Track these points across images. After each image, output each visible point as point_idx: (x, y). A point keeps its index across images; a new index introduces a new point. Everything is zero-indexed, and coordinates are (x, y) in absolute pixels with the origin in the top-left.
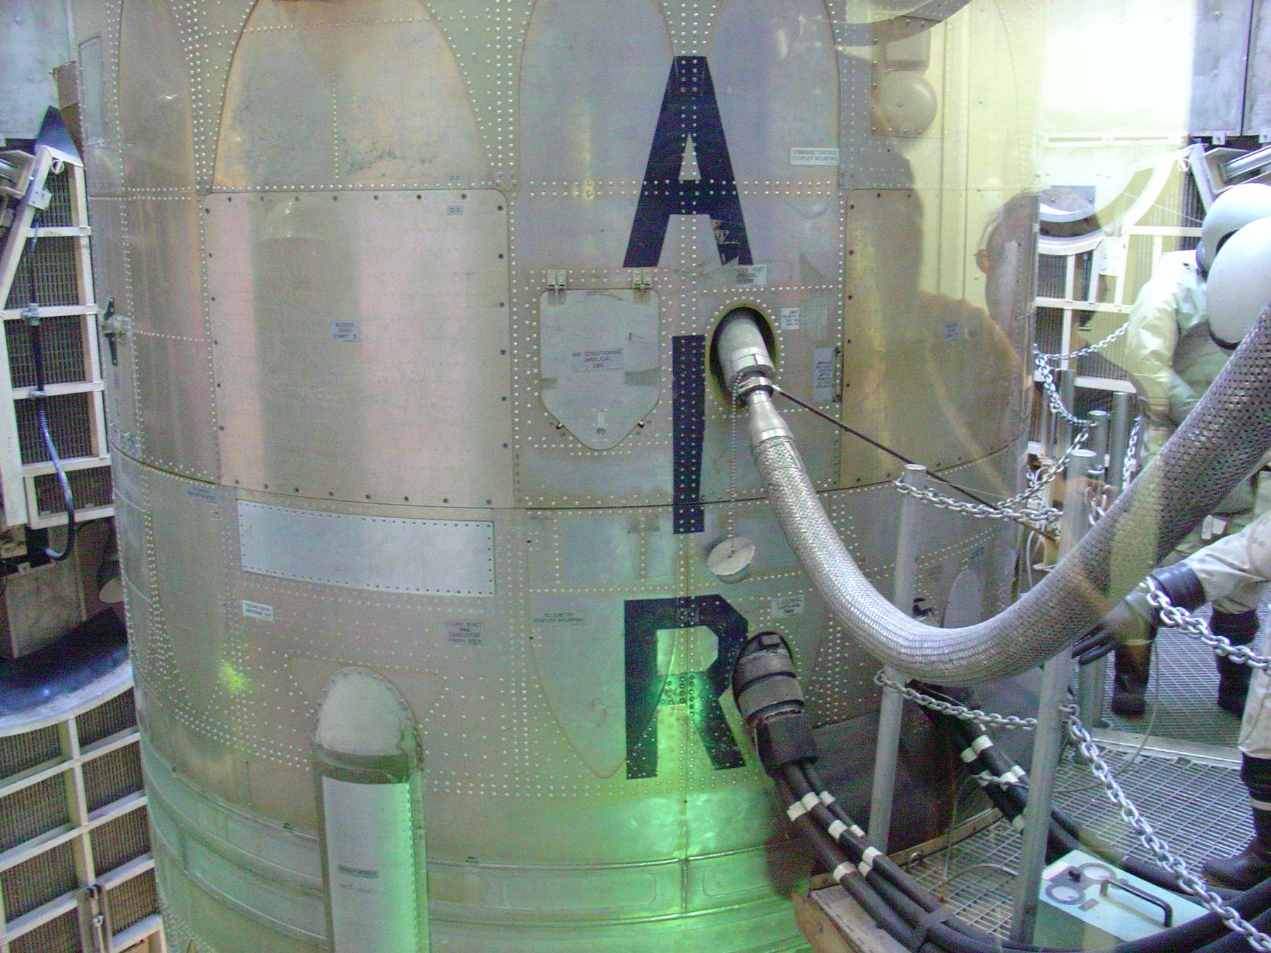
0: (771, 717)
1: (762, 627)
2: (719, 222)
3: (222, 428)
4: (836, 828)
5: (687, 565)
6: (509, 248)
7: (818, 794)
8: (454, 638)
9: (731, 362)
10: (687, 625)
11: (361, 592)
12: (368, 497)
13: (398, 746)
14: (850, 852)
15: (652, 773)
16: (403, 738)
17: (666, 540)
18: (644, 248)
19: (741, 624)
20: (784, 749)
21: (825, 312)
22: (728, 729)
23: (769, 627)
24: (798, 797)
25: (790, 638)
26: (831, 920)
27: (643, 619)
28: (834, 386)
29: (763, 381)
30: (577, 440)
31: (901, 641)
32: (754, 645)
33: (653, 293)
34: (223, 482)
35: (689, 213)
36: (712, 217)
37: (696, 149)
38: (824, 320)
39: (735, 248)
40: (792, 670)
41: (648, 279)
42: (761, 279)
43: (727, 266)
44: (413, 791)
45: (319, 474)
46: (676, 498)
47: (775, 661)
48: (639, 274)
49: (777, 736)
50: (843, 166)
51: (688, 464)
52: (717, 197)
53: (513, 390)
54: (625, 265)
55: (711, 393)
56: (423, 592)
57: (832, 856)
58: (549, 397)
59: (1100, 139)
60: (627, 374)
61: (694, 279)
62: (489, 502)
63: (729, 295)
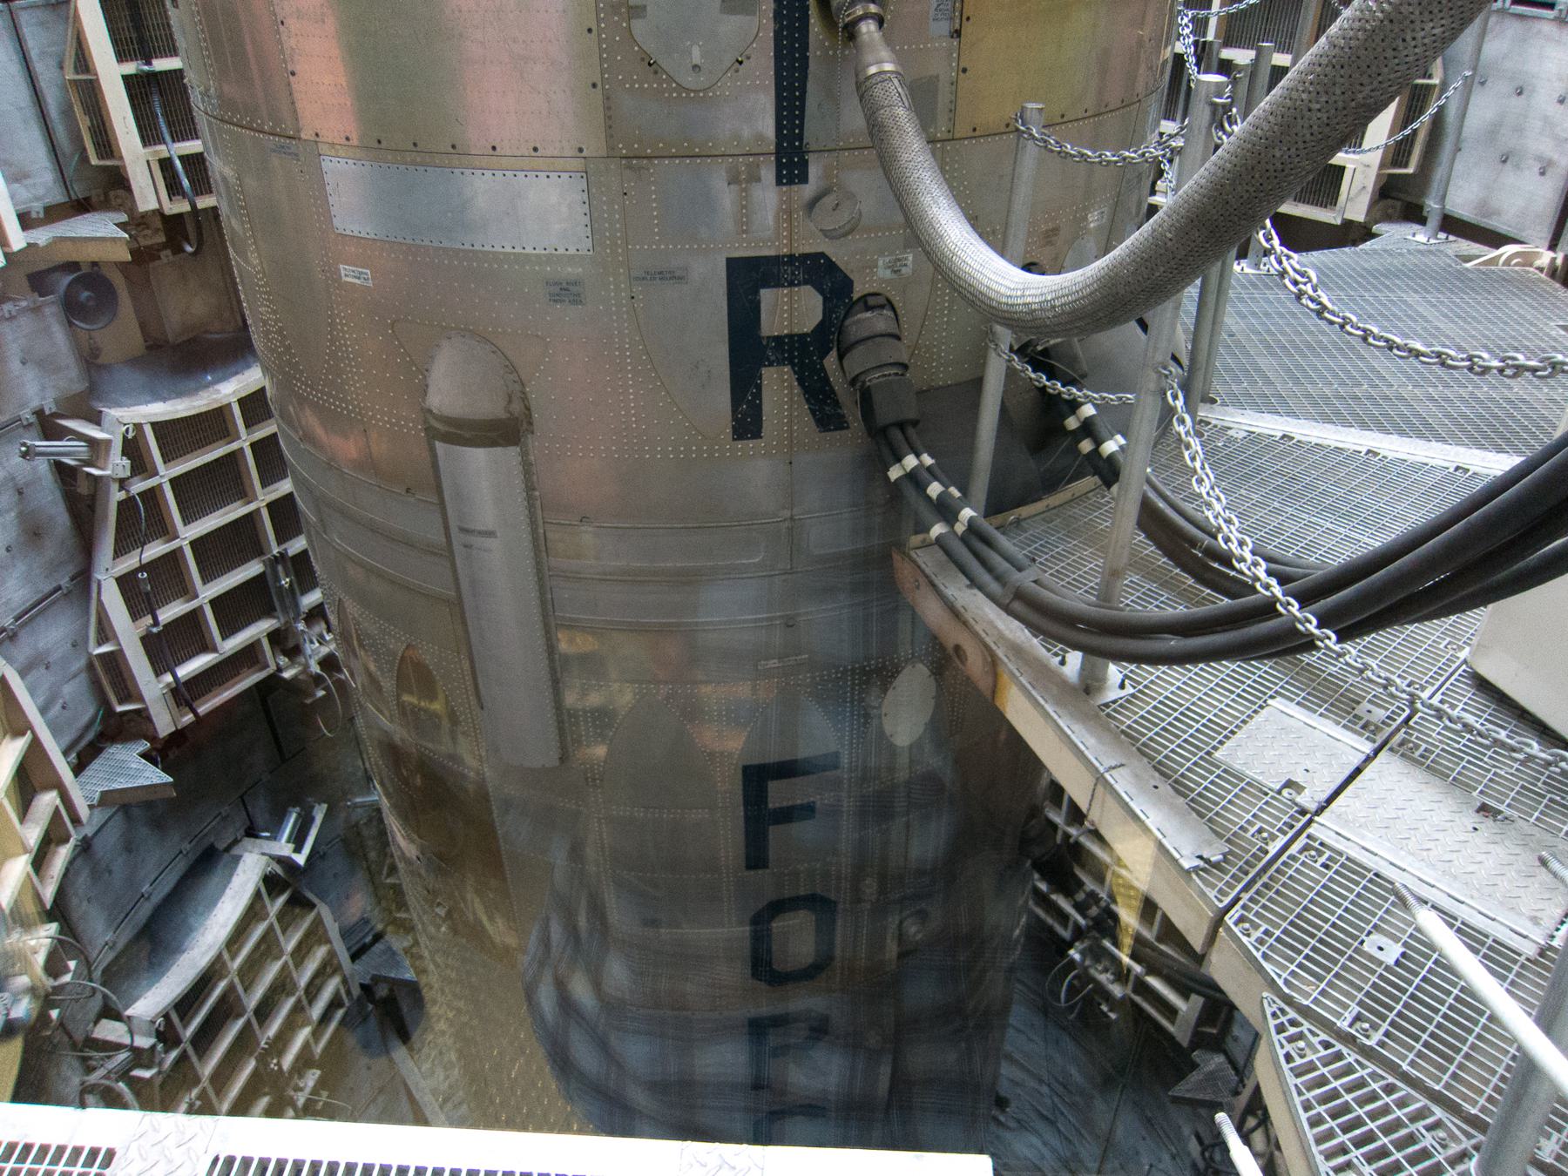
0: (874, 379)
1: (868, 289)
3: (293, 74)
4: (935, 489)
5: (790, 220)
7: (918, 456)
8: (555, 299)
10: (791, 284)
11: (457, 251)
12: (454, 147)
13: (507, 409)
14: (946, 510)
15: (757, 434)
16: (510, 401)
17: (768, 195)
19: (848, 283)
20: (886, 413)
22: (833, 392)
23: (875, 288)
24: (899, 459)
25: (896, 300)
26: (927, 576)
27: (748, 278)
28: (952, 19)
30: (671, 79)
31: (1003, 290)
32: (861, 304)
34: (303, 136)
40: (896, 331)
44: (524, 454)
45: (411, 129)
46: (779, 145)
47: (878, 322)
49: (877, 398)
56: (518, 250)
57: (926, 513)
58: (638, 26)
62: (581, 150)
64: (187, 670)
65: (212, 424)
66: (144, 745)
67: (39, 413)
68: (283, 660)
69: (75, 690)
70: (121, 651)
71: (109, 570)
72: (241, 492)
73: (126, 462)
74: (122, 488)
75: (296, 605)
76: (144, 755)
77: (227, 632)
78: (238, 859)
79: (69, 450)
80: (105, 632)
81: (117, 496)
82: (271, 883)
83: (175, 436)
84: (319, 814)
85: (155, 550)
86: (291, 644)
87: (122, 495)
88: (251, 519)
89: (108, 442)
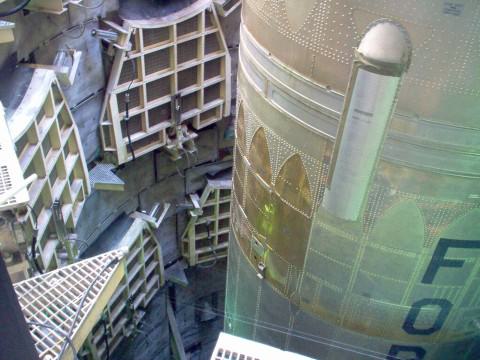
8: (447, 11)
16: (404, 56)
44: (400, 81)
64: (135, 137)
65: (163, 34)
66: (113, 167)
67: (99, 17)
68: (169, 141)
69: (92, 137)
70: (112, 126)
71: (116, 88)
72: (166, 64)
73: (131, 45)
74: (126, 55)
75: (179, 118)
76: (112, 170)
77: (152, 124)
78: (133, 220)
79: (107, 35)
80: (108, 117)
81: (124, 59)
82: (145, 232)
83: (151, 35)
84: (167, 207)
85: (134, 84)
86: (172, 134)
87: (125, 59)
88: (168, 79)
89: (126, 35)
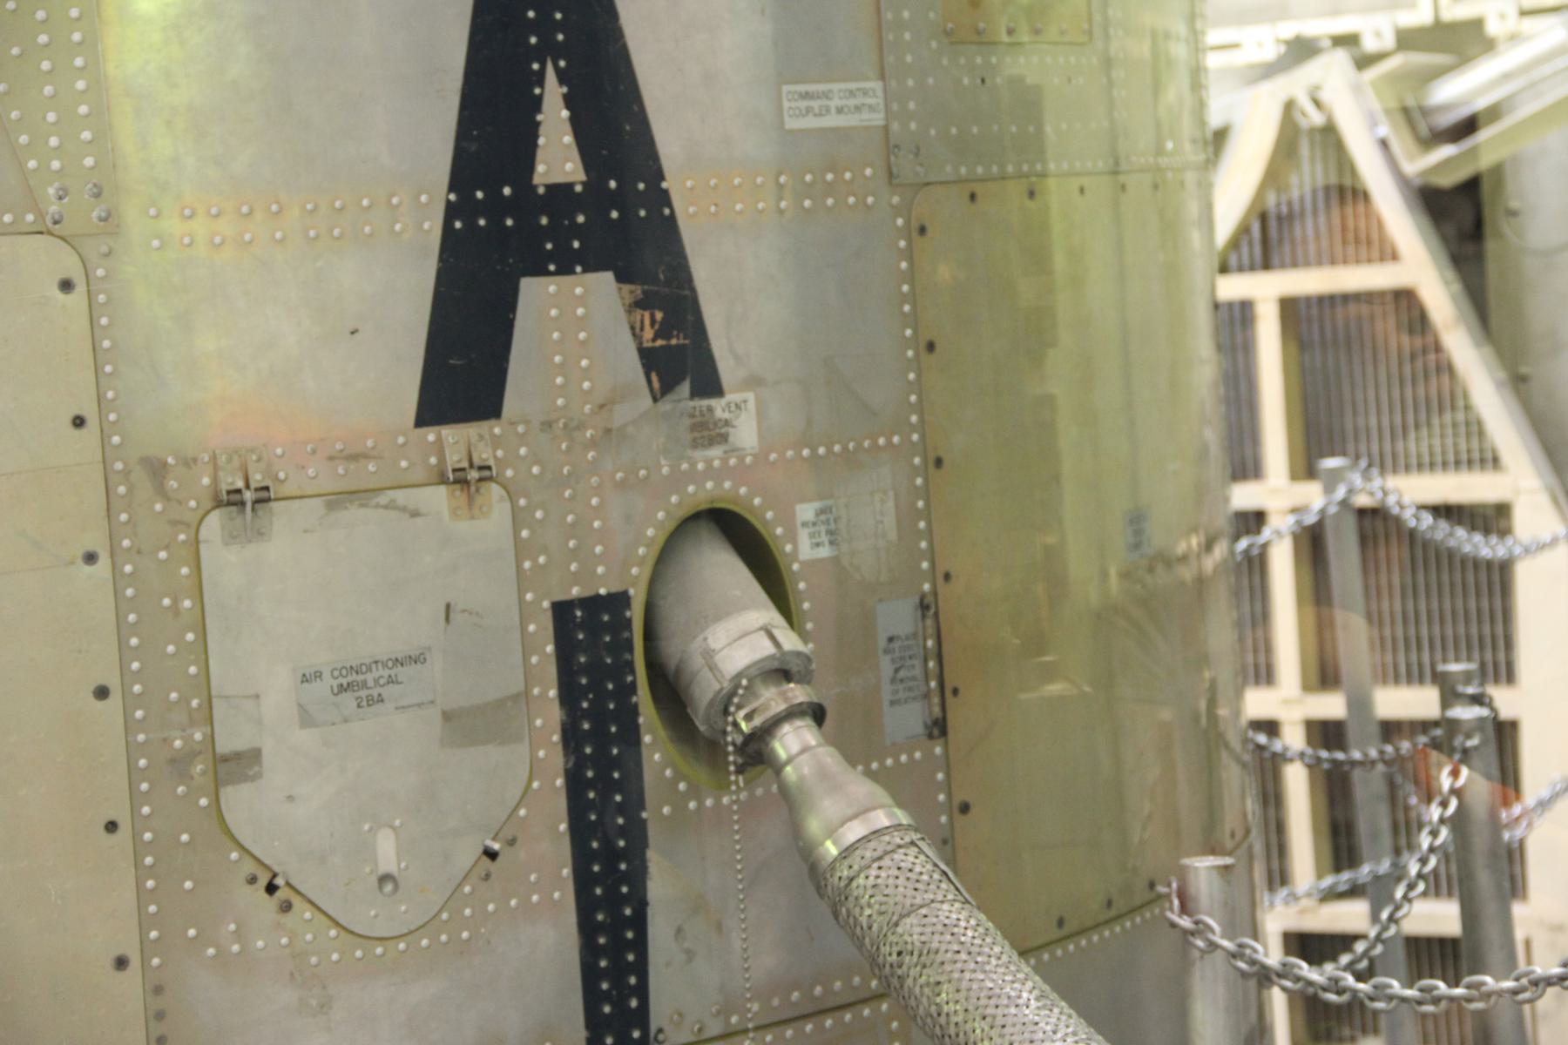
2: (638, 290)
6: (100, 398)
9: (697, 661)
18: (464, 371)
21: (891, 504)
28: (926, 696)
29: (798, 693)
33: (495, 490)
35: (565, 270)
36: (621, 278)
37: (569, 101)
38: (890, 522)
39: (679, 359)
41: (483, 454)
42: (746, 434)
43: (666, 406)
48: (455, 440)
50: (895, 126)
51: (617, 948)
52: (626, 227)
53: (135, 799)
54: (421, 421)
55: (657, 750)
58: (239, 801)
59: (1235, 46)
60: (447, 716)
61: (593, 444)
63: (677, 481)
